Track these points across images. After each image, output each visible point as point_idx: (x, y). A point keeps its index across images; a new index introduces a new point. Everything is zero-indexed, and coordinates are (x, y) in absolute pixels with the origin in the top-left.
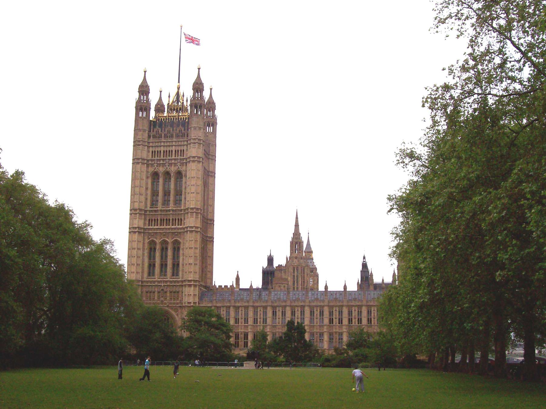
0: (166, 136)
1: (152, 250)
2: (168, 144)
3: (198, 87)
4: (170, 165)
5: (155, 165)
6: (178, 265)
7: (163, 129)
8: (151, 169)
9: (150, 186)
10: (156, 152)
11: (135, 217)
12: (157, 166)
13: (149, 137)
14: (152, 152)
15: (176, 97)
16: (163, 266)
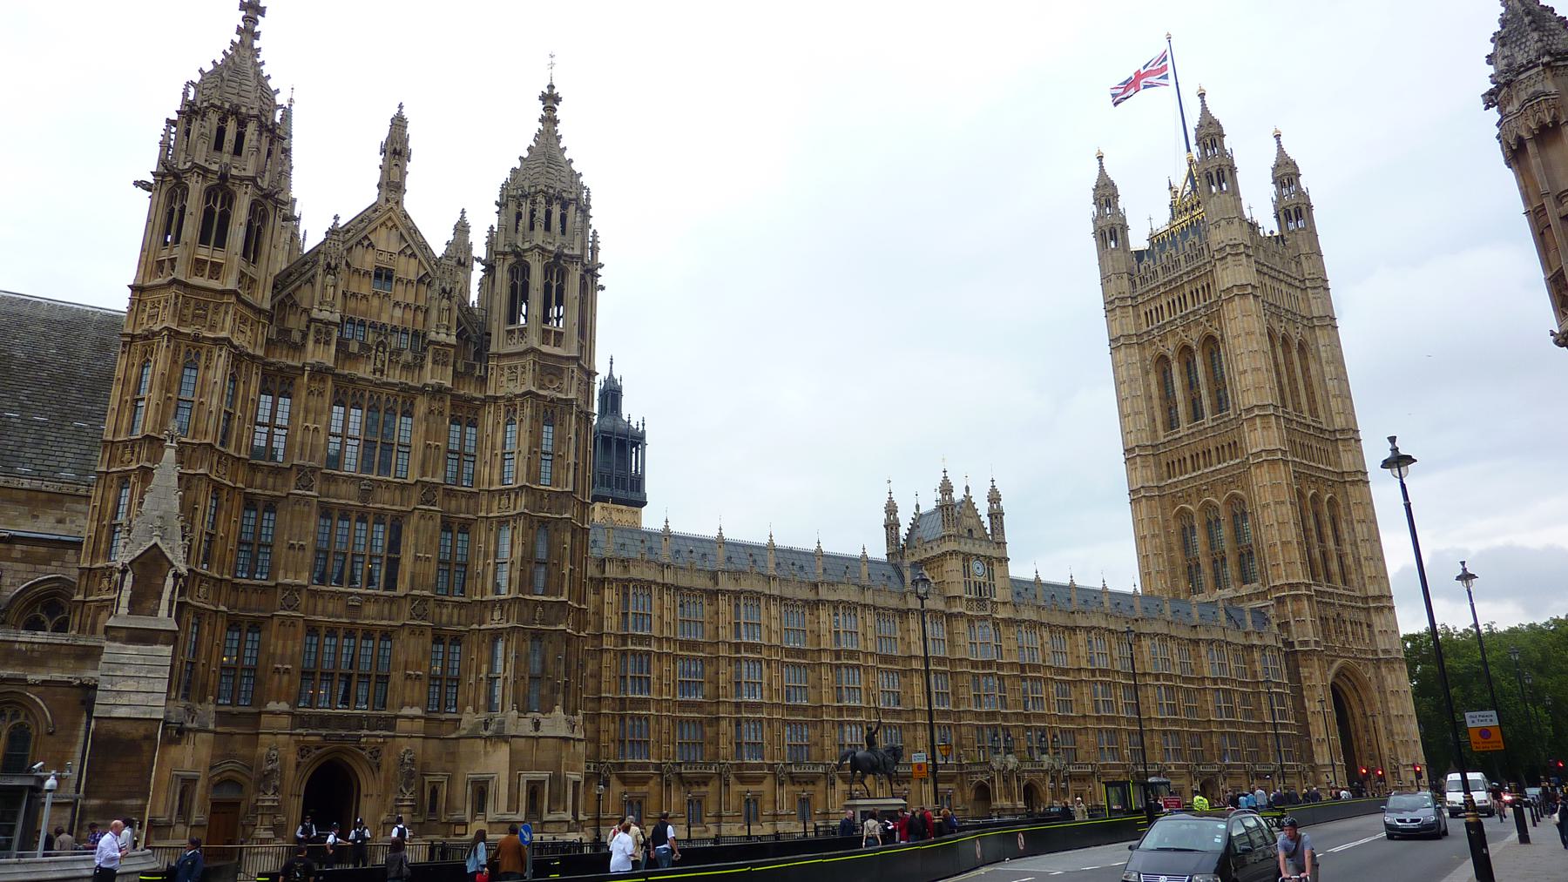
0: (1165, 269)
1: (1186, 533)
2: (1174, 285)
3: (1210, 134)
4: (1187, 328)
6: (1251, 553)
7: (1158, 257)
8: (1148, 354)
9: (1154, 389)
10: (1154, 312)
11: (1133, 467)
13: (1134, 283)
14: (1146, 313)
15: (1189, 183)
16: (1218, 562)
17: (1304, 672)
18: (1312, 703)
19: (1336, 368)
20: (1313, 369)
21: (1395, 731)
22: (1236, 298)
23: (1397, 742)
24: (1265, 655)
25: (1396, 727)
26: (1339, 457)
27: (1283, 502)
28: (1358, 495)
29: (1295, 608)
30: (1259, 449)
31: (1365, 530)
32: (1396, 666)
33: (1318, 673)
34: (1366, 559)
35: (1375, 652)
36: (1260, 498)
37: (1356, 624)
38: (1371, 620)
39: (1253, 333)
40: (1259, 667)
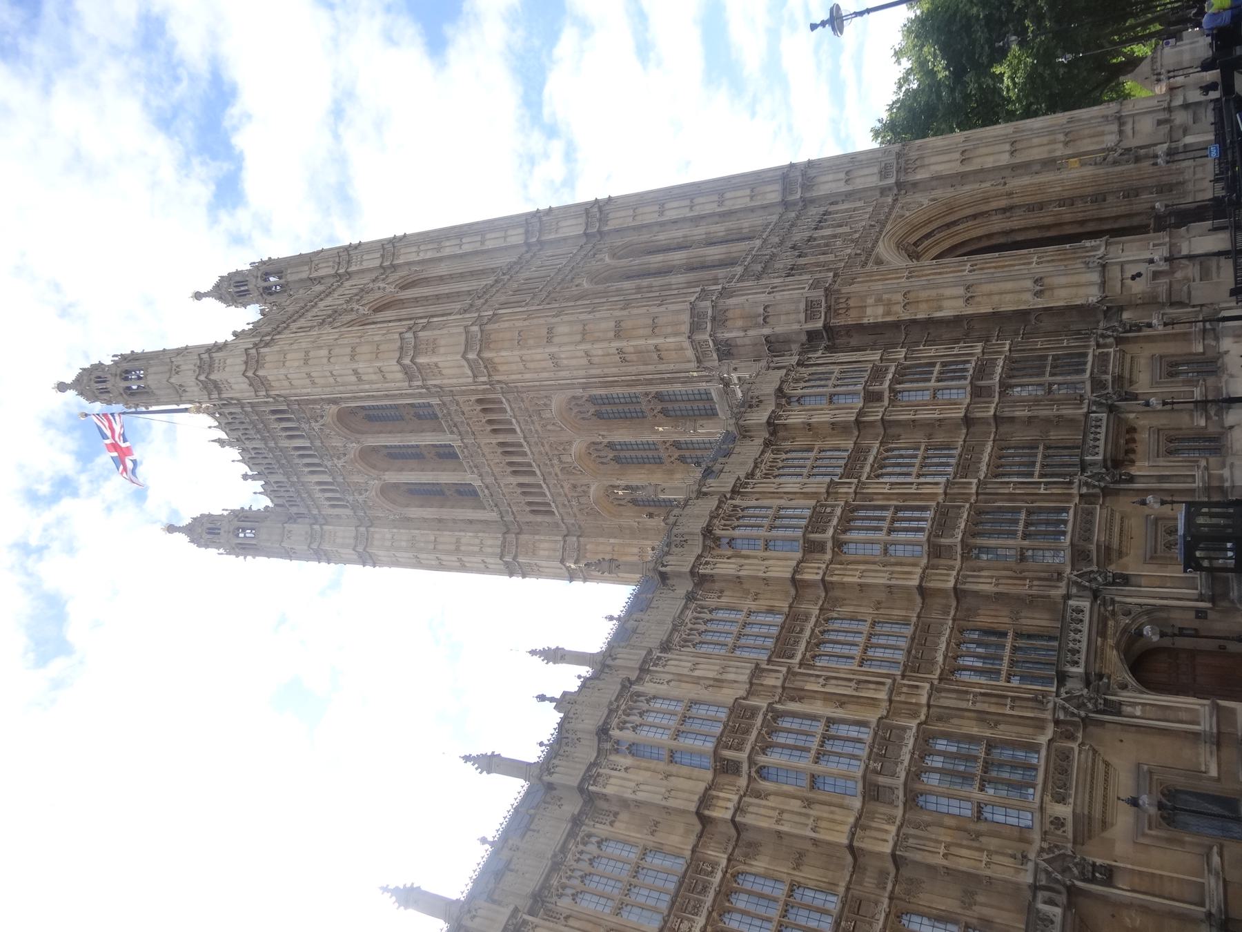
5: (361, 499)
6: (659, 397)
12: (361, 494)
13: (300, 515)
14: (333, 506)
17: (875, 314)
18: (946, 303)
19: (448, 239)
20: (443, 269)
21: (1045, 156)
22: (260, 373)
23: (1069, 151)
24: (799, 399)
25: (1037, 154)
26: (565, 239)
27: (550, 330)
28: (623, 214)
29: (740, 323)
30: (465, 363)
31: (675, 204)
32: (913, 155)
33: (878, 286)
34: (721, 203)
35: (884, 191)
36: (544, 369)
37: (826, 220)
38: (827, 197)
39: (307, 353)
40: (823, 417)
